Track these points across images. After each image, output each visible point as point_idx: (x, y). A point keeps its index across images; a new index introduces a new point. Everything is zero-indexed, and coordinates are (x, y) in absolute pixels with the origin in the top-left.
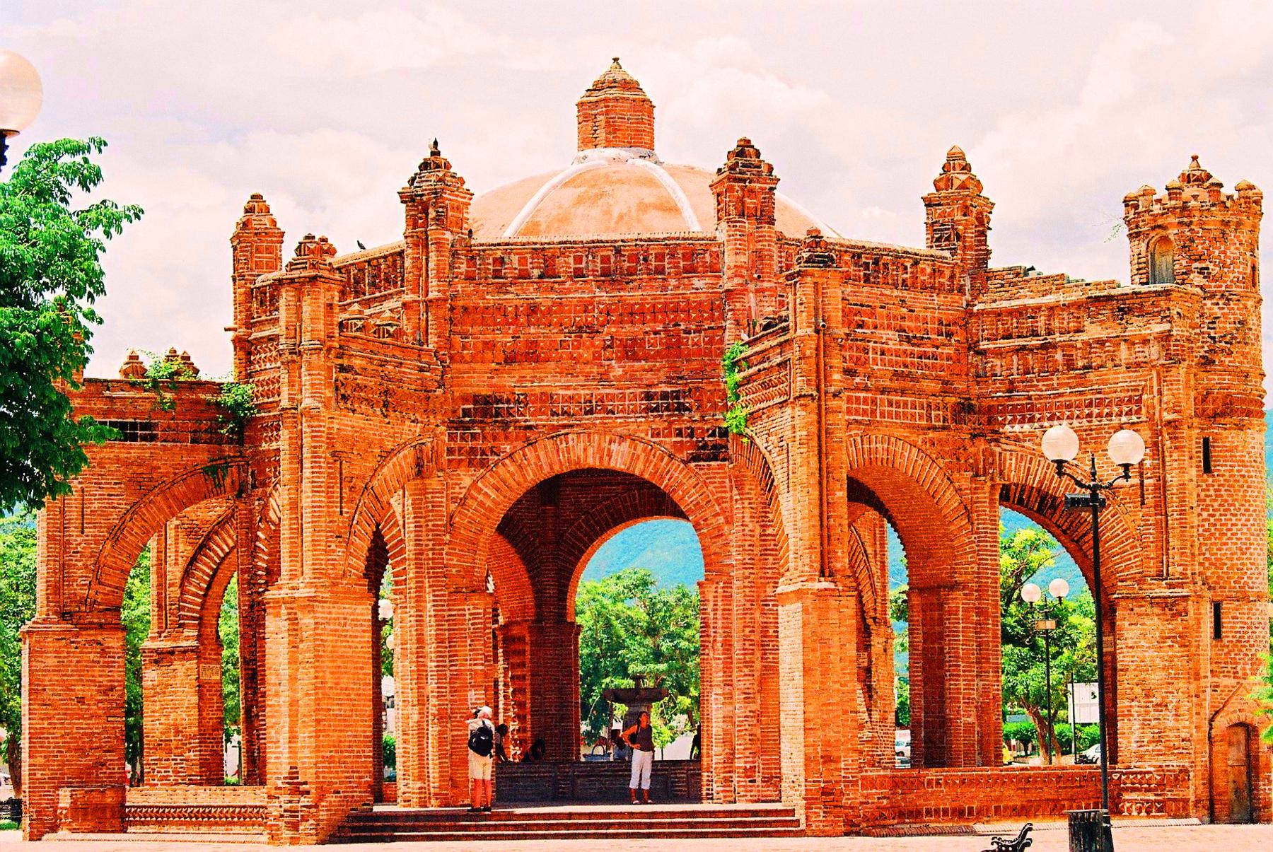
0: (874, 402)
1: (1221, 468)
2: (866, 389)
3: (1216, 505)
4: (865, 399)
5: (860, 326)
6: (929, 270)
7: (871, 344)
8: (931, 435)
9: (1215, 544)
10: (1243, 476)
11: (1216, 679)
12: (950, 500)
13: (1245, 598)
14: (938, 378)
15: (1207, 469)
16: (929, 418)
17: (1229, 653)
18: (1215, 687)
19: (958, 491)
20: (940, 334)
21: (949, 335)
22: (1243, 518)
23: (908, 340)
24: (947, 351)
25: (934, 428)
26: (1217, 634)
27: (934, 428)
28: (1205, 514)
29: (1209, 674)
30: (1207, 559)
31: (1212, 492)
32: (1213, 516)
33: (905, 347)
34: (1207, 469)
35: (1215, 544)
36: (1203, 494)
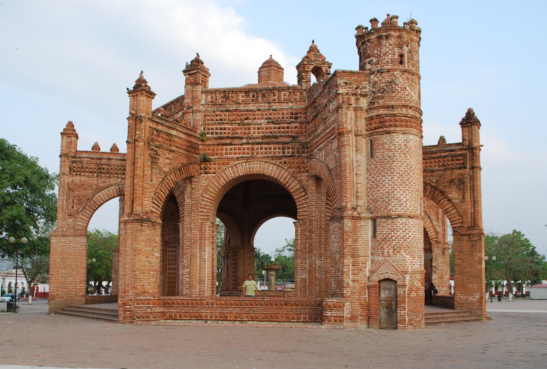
0: (253, 149)
1: (378, 154)
2: (248, 144)
3: (375, 172)
4: (248, 149)
5: (246, 119)
6: (288, 94)
7: (252, 126)
8: (284, 160)
9: (374, 191)
10: (390, 157)
11: (373, 257)
12: (293, 186)
13: (389, 217)
14: (289, 136)
15: (372, 156)
16: (284, 153)
17: (379, 244)
18: (373, 261)
19: (300, 182)
20: (291, 118)
21: (296, 118)
22: (390, 177)
23: (273, 123)
24: (295, 125)
25: (287, 157)
26: (374, 236)
27: (287, 157)
28: (370, 177)
29: (370, 255)
30: (370, 199)
31: (373, 166)
32: (373, 177)
33: (271, 125)
34: (372, 156)
35: (374, 191)
36: (369, 168)
